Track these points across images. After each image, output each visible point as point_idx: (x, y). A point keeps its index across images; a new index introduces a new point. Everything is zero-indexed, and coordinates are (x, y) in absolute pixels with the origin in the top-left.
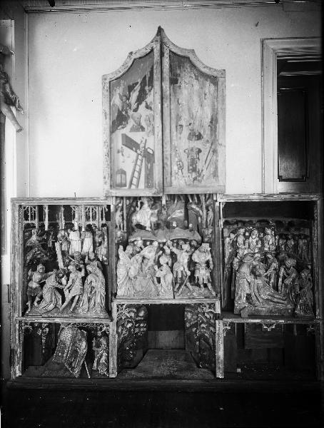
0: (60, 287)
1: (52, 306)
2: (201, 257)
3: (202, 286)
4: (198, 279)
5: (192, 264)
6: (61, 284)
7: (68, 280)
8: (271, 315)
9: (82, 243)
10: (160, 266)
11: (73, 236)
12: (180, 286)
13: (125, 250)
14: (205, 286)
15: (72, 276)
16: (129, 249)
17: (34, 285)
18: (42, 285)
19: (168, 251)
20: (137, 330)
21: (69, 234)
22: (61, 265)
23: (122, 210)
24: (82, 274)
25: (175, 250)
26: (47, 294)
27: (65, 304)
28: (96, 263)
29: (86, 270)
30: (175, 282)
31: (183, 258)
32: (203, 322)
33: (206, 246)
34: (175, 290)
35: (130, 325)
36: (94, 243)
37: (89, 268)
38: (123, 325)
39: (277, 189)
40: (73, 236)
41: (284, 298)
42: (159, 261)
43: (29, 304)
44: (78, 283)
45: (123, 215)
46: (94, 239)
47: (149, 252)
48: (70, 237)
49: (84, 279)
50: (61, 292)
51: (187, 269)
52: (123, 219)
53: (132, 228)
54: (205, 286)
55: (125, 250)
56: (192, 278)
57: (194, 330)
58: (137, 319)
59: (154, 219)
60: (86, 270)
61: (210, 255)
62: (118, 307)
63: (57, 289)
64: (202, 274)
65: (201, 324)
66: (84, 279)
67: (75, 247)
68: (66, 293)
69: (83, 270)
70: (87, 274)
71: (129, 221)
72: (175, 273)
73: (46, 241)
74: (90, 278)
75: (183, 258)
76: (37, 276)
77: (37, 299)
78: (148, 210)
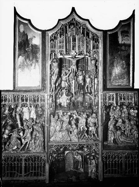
0: (19, 137)
2: (91, 120)
6: (20, 135)
7: (23, 134)
8: (125, 148)
9: (30, 113)
14: (94, 135)
15: (26, 131)
16: (56, 117)
19: (75, 117)
21: (23, 109)
22: (20, 126)
23: (53, 97)
26: (13, 140)
27: (23, 146)
28: (40, 125)
30: (78, 134)
31: (82, 121)
33: (94, 115)
36: (36, 112)
37: (35, 127)
38: (52, 155)
39: (135, 88)
40: (25, 110)
42: (71, 123)
44: (29, 135)
45: (52, 100)
47: (66, 119)
48: (24, 111)
50: (20, 139)
51: (85, 127)
52: (53, 102)
53: (58, 106)
56: (87, 132)
57: (88, 157)
59: (68, 101)
63: (18, 138)
65: (92, 153)
66: (32, 133)
67: (26, 116)
68: (23, 140)
71: (56, 102)
72: (79, 129)
73: (12, 113)
74: (35, 133)
75: (82, 121)
77: (8, 144)
78: (66, 96)
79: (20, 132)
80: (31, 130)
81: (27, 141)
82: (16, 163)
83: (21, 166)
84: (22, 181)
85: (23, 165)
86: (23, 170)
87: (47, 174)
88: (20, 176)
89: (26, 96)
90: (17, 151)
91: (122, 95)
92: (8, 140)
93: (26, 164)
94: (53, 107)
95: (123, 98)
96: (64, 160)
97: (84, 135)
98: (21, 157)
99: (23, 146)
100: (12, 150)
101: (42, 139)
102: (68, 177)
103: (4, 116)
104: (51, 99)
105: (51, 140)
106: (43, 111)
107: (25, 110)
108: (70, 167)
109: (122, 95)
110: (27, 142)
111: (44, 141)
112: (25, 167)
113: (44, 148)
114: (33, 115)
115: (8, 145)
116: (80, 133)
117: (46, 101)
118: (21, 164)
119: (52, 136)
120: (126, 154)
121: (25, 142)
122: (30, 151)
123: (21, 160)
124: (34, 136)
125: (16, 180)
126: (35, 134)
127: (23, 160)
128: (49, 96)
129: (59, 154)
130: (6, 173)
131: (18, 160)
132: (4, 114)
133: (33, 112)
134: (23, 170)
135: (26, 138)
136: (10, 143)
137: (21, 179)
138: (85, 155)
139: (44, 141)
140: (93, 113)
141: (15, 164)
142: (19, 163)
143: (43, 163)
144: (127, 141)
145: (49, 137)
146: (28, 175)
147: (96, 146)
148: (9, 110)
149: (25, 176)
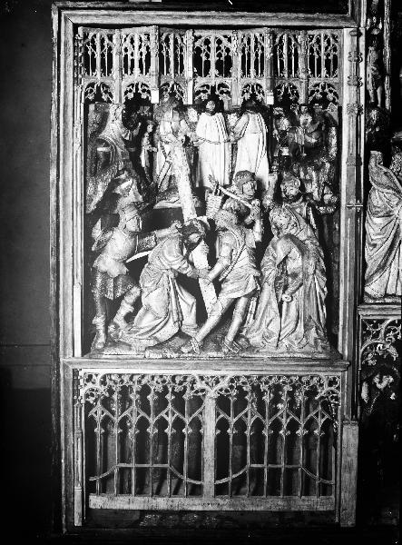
0: (188, 272)
1: (171, 329)
7: (212, 260)
9: (234, 148)
13: (387, 162)
17: (110, 263)
18: (135, 269)
21: (192, 126)
24: (256, 235)
26: (154, 293)
29: (267, 224)
37: (278, 217)
38: (370, 381)
43: (99, 321)
44: (245, 260)
45: (379, 63)
46: (269, 135)
48: (200, 131)
49: (258, 253)
55: (387, 162)
66: (258, 253)
67: (214, 166)
68: (208, 292)
69: (258, 227)
70: (267, 236)
74: (280, 248)
76: (118, 244)
77: (126, 308)
79: (191, 246)
80: (258, 238)
81: (235, 295)
82: (170, 419)
83: (198, 438)
84: (202, 514)
85: (210, 432)
86: (209, 455)
87: (349, 479)
89: (219, 42)
90: (178, 351)
93: (222, 425)
98: (199, 385)
100: (152, 343)
101: (319, 284)
103: (100, 149)
104: (373, 55)
105: (373, 288)
106: (327, 125)
107: (208, 127)
110: (236, 300)
111: (331, 301)
112: (221, 441)
113: (332, 339)
114: (253, 154)
115: (129, 318)
117: (346, 66)
118: (197, 424)
119: (382, 268)
121: (224, 300)
122: (251, 348)
123: (198, 402)
124: (270, 273)
126: (281, 256)
127: (210, 406)
128: (362, 39)
130: (112, 475)
131: (179, 404)
132: (104, 142)
133: (253, 130)
134: (209, 455)
135: (225, 280)
136: (137, 304)
137: (195, 505)
139: (331, 301)
141: (162, 424)
142: (187, 420)
143: (321, 421)
145: (360, 280)
146: (237, 487)
148: (126, 122)
149: (220, 490)
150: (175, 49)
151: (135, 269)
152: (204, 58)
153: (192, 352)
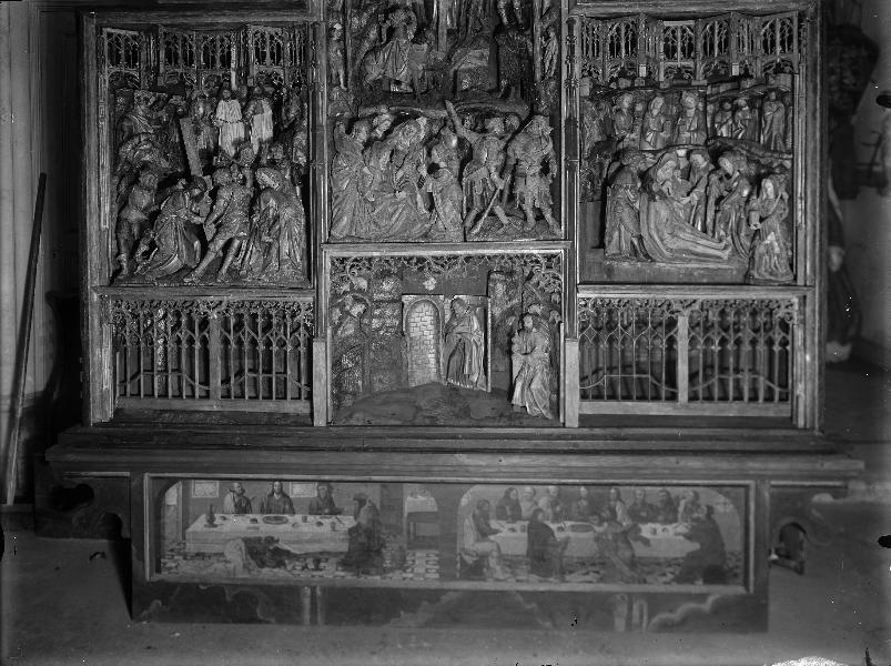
2: (532, 151)
3: (531, 215)
4: (523, 201)
5: (510, 169)
10: (433, 169)
11: (228, 111)
12: (478, 217)
15: (224, 194)
18: (153, 217)
20: (376, 323)
25: (472, 138)
27: (211, 257)
29: (255, 184)
32: (537, 303)
34: (468, 224)
35: (358, 309)
36: (276, 116)
41: (723, 244)
43: (123, 256)
51: (495, 177)
54: (540, 217)
58: (376, 297)
60: (255, 184)
61: (551, 146)
62: (333, 263)
64: (533, 189)
66: (252, 205)
68: (209, 232)
77: (144, 248)
84: (208, 413)
88: (207, 396)
91: (679, 34)
92: (141, 235)
94: (346, 85)
95: (683, 50)
96: (401, 333)
97: (492, 214)
99: (211, 257)
102: (419, 409)
108: (426, 364)
109: (679, 34)
114: (263, 128)
115: (146, 254)
116: (475, 213)
120: (696, 307)
125: (184, 412)
129: (379, 303)
130: (132, 379)
137: (206, 406)
138: (497, 312)
140: (533, 114)
144: (700, 249)
147: (549, 267)
150: (183, 46)
151: (153, 217)
152: (211, 54)
153: (192, 282)
